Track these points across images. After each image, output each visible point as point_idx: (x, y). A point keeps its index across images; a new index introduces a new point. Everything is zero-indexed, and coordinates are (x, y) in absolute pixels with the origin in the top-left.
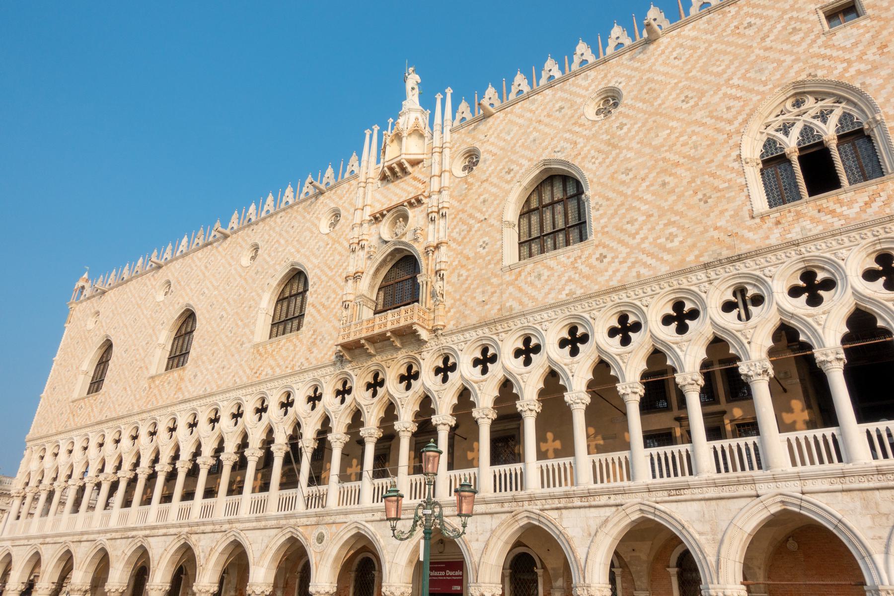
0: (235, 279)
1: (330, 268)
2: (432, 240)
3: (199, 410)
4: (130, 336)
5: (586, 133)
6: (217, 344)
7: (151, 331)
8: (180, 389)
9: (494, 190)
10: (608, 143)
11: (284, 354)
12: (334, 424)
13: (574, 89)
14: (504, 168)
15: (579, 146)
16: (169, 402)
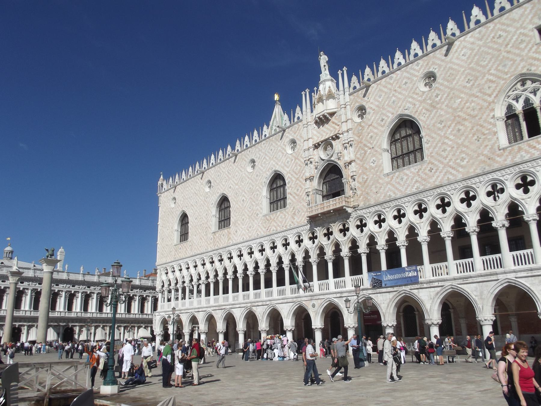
0: (246, 180)
1: (296, 173)
2: (347, 159)
3: (242, 248)
4: (196, 211)
5: (420, 98)
6: (244, 215)
7: (207, 208)
8: (230, 238)
9: (376, 131)
10: (431, 105)
11: (281, 220)
12: (311, 254)
13: (412, 71)
14: (379, 118)
15: (417, 106)
16: (226, 245)
